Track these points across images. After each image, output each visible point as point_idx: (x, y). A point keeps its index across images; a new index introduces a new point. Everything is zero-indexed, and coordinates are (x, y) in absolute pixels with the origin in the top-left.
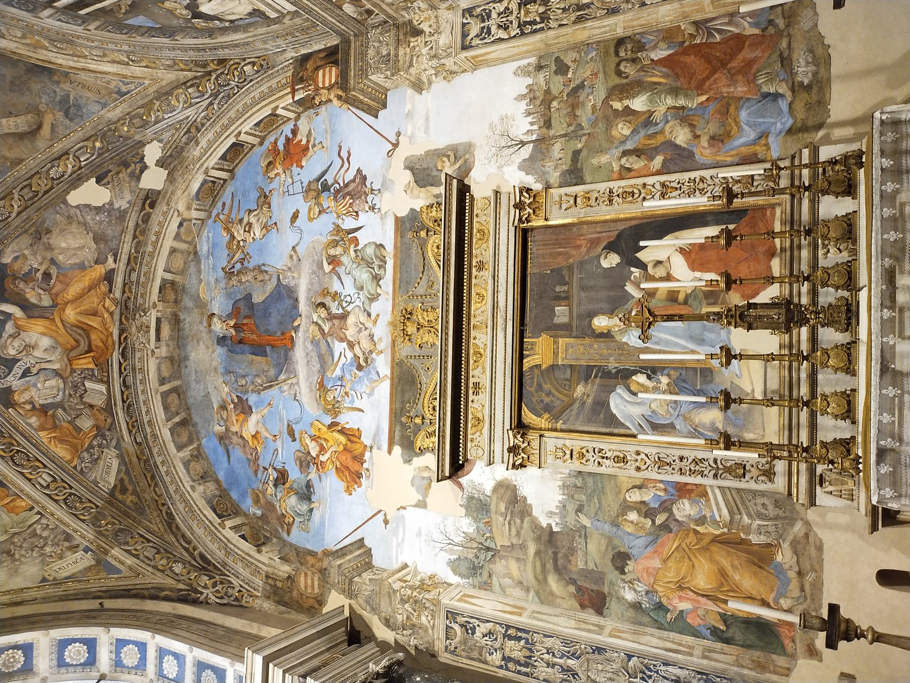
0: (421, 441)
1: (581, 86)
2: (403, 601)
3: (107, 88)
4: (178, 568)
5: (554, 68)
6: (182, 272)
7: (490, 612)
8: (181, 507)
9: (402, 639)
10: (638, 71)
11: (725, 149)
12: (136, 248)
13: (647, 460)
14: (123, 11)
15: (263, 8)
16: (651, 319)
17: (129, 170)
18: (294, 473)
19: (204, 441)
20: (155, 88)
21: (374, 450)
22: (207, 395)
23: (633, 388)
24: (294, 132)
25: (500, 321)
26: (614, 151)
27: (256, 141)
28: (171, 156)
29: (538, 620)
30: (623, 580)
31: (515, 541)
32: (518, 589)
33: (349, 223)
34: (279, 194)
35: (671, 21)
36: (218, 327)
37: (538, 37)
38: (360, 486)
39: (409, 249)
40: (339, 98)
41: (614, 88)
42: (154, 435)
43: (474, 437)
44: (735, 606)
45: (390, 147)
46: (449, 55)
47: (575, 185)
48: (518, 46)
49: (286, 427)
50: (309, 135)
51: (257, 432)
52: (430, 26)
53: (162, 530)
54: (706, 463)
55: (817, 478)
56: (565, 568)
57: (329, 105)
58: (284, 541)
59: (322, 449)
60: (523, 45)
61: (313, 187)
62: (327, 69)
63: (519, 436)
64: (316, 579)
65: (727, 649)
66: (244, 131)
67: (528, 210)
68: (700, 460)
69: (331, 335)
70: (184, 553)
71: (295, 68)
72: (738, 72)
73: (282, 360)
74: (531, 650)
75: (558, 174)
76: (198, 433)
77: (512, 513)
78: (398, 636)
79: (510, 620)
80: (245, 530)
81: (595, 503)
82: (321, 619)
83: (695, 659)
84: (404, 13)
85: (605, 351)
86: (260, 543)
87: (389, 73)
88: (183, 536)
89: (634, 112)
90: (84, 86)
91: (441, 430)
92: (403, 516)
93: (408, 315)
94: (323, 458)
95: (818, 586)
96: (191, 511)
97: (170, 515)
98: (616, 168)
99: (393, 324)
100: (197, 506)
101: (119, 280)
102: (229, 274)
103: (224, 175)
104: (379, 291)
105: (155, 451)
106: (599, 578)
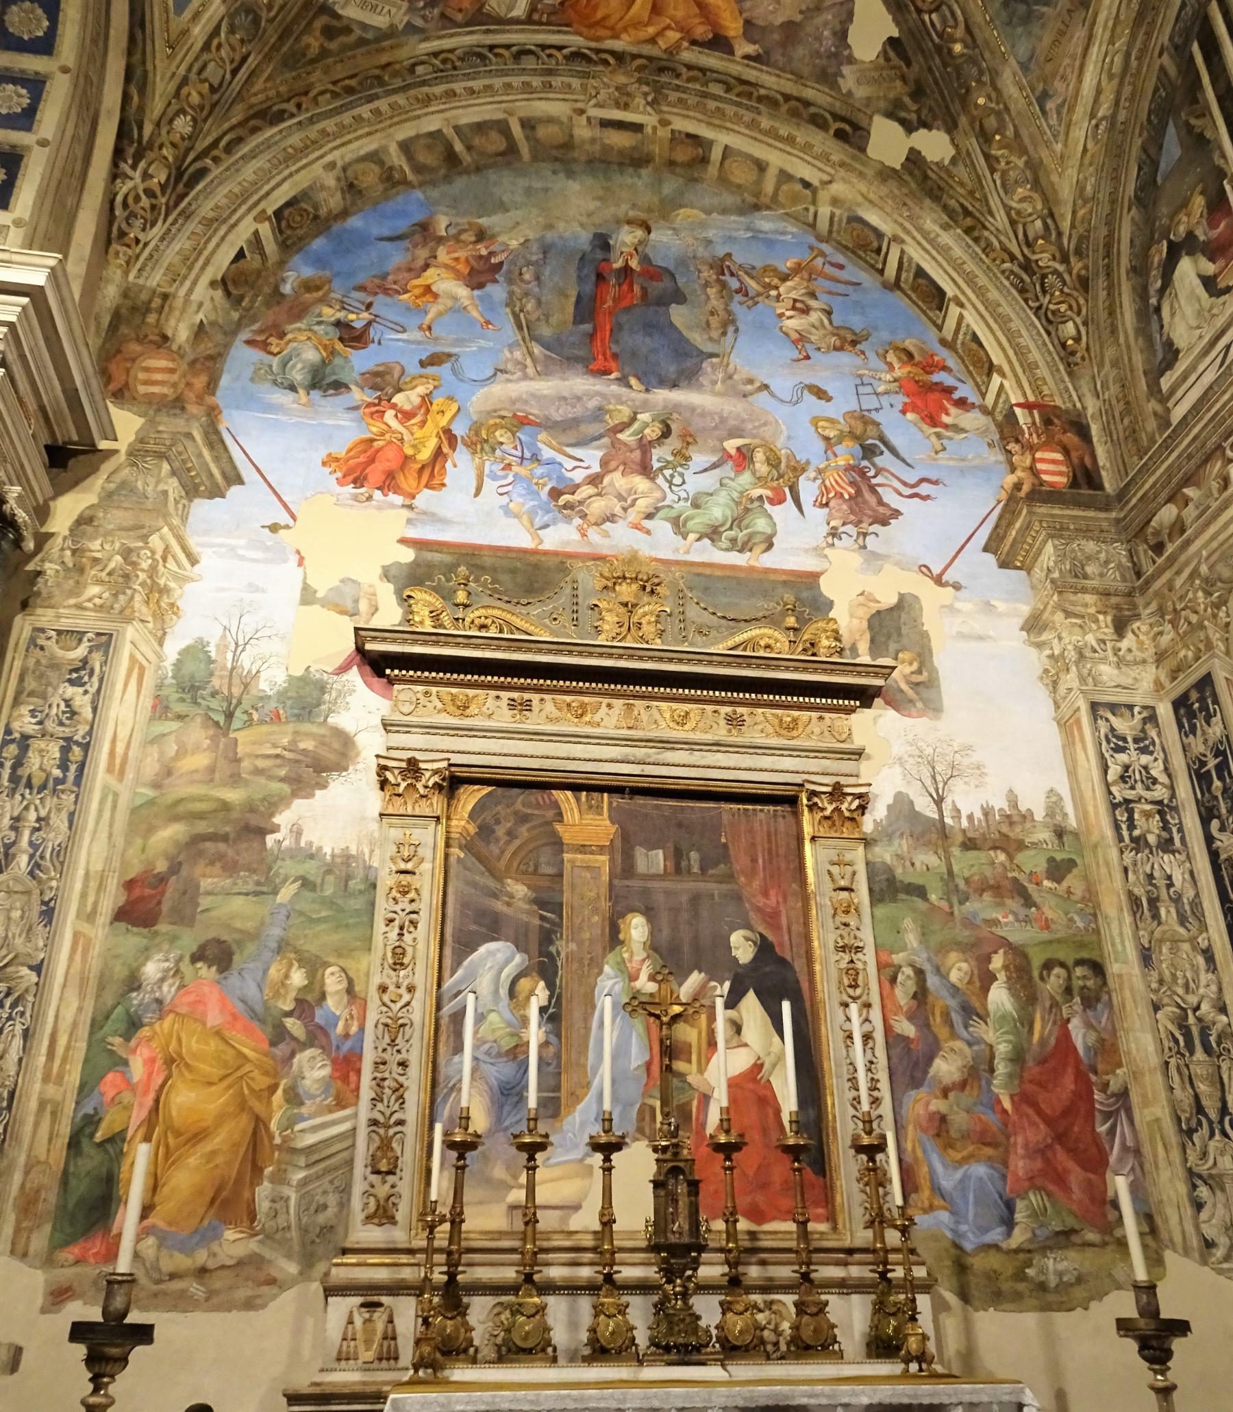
0: (424, 601)
1: (1028, 902)
2: (127, 553)
3: (1054, 75)
4: (183, 125)
5: (1059, 857)
6: (723, 180)
7: (112, 715)
8: (295, 139)
9: (55, 546)
10: (1052, 998)
11: (925, 1138)
12: (767, 97)
13: (399, 1005)
14: (1193, 121)
15: (1181, 367)
16: (665, 1019)
17: (907, 100)
18: (360, 361)
19: (418, 194)
21: (406, 513)
22: (503, 207)
23: (524, 984)
24: (962, 403)
25: (640, 753)
26: (924, 955)
28: (926, 177)
29: (102, 802)
30: (180, 959)
31: (246, 764)
32: (157, 767)
33: (808, 489)
34: (859, 368)
35: (1129, 1053)
36: (627, 237)
37: (1109, 832)
38: (340, 482)
39: (765, 595)
40: (1018, 486)
41: (1025, 956)
42: (427, 100)
43: (434, 698)
44: (141, 1156)
45: (936, 570)
46: (1083, 680)
47: (871, 890)
48: (1095, 798)
49: (447, 350)
50: (957, 429)
51: (436, 296)
52: (1130, 650)
53: (254, 100)
54: (396, 1107)
55: (376, 1299)
56: (200, 854)
57: (1004, 467)
58: (234, 333)
59: (406, 416)
60: (1096, 807)
62: (1063, 469)
63: (436, 779)
64: (165, 390)
65: (59, 1145)
66: (965, 313)
67: (830, 808)
68: (402, 1097)
69: (613, 444)
70: (209, 140)
71: (1067, 411)
72: (1047, 1161)
74: (43, 787)
75: (888, 858)
76: (433, 183)
77: (297, 761)
78: (60, 540)
79: (100, 752)
81: (319, 912)
82: (98, 397)
83: (37, 1086)
84: (1154, 606)
85: (587, 935)
86: (231, 288)
87: (1056, 575)
88: (240, 140)
89: (985, 990)
90: (1062, 33)
91: (449, 639)
92: (285, 561)
93: (649, 587)
94: (389, 415)
95: (182, 1303)
96: (288, 159)
97: (280, 117)
98: (898, 958)
99: (633, 558)
100: (297, 171)
101: (711, 60)
102: (721, 266)
104: (692, 536)
105: (400, 99)
106: (185, 915)
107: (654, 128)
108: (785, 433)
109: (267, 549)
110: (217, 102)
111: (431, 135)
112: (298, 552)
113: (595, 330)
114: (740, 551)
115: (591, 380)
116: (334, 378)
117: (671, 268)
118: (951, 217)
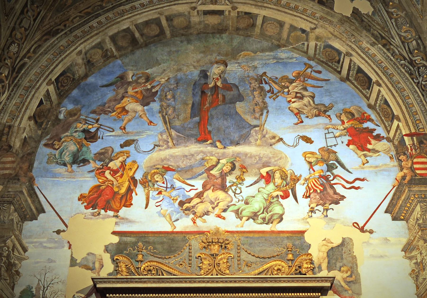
4: (14, 48)
19: (119, 62)
20: (415, 13)
21: (115, 220)
22: (158, 63)
24: (378, 138)
27: (372, 101)
28: (363, 21)
33: (300, 189)
38: (86, 208)
40: (404, 178)
42: (122, 14)
45: (361, 225)
49: (132, 138)
50: (375, 151)
51: (127, 112)
53: (44, 28)
57: (397, 169)
58: (39, 141)
59: (114, 172)
61: (332, 156)
66: (381, 89)
69: (208, 176)
70: (26, 50)
73: (188, 132)
76: (125, 55)
80: (47, 105)
86: (37, 119)
88: (39, 46)
92: (63, 247)
93: (224, 245)
96: (61, 52)
97: (57, 32)
99: (217, 232)
100: (65, 58)
102: (260, 79)
103: (344, 72)
104: (244, 219)
105: (110, 15)
107: (229, 12)
108: (290, 162)
109: (56, 242)
110: (28, 35)
111: (124, 30)
112: (69, 242)
113: (200, 120)
114: (267, 224)
115: (199, 145)
116: (83, 157)
117: (237, 84)
118: (376, 40)
